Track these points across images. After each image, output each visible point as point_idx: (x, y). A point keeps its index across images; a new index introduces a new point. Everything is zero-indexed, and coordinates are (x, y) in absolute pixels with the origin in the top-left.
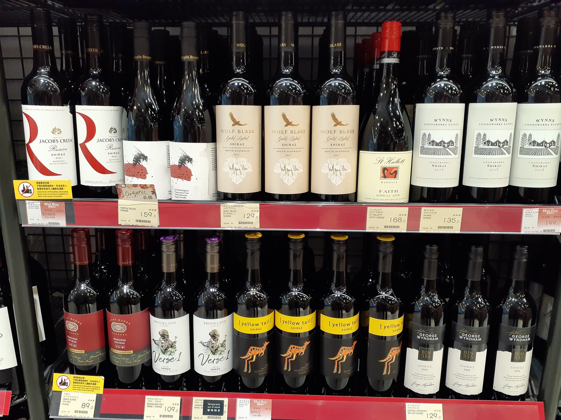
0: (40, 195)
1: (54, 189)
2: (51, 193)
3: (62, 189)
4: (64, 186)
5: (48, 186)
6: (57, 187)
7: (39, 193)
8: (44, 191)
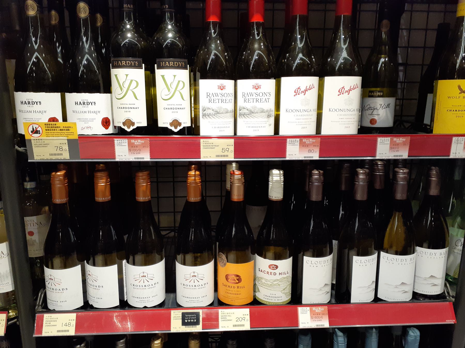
0: (49, 136)
1: (61, 130)
2: (58, 134)
3: (69, 130)
4: (70, 127)
5: (56, 127)
6: (64, 129)
7: (47, 134)
8: (51, 131)
